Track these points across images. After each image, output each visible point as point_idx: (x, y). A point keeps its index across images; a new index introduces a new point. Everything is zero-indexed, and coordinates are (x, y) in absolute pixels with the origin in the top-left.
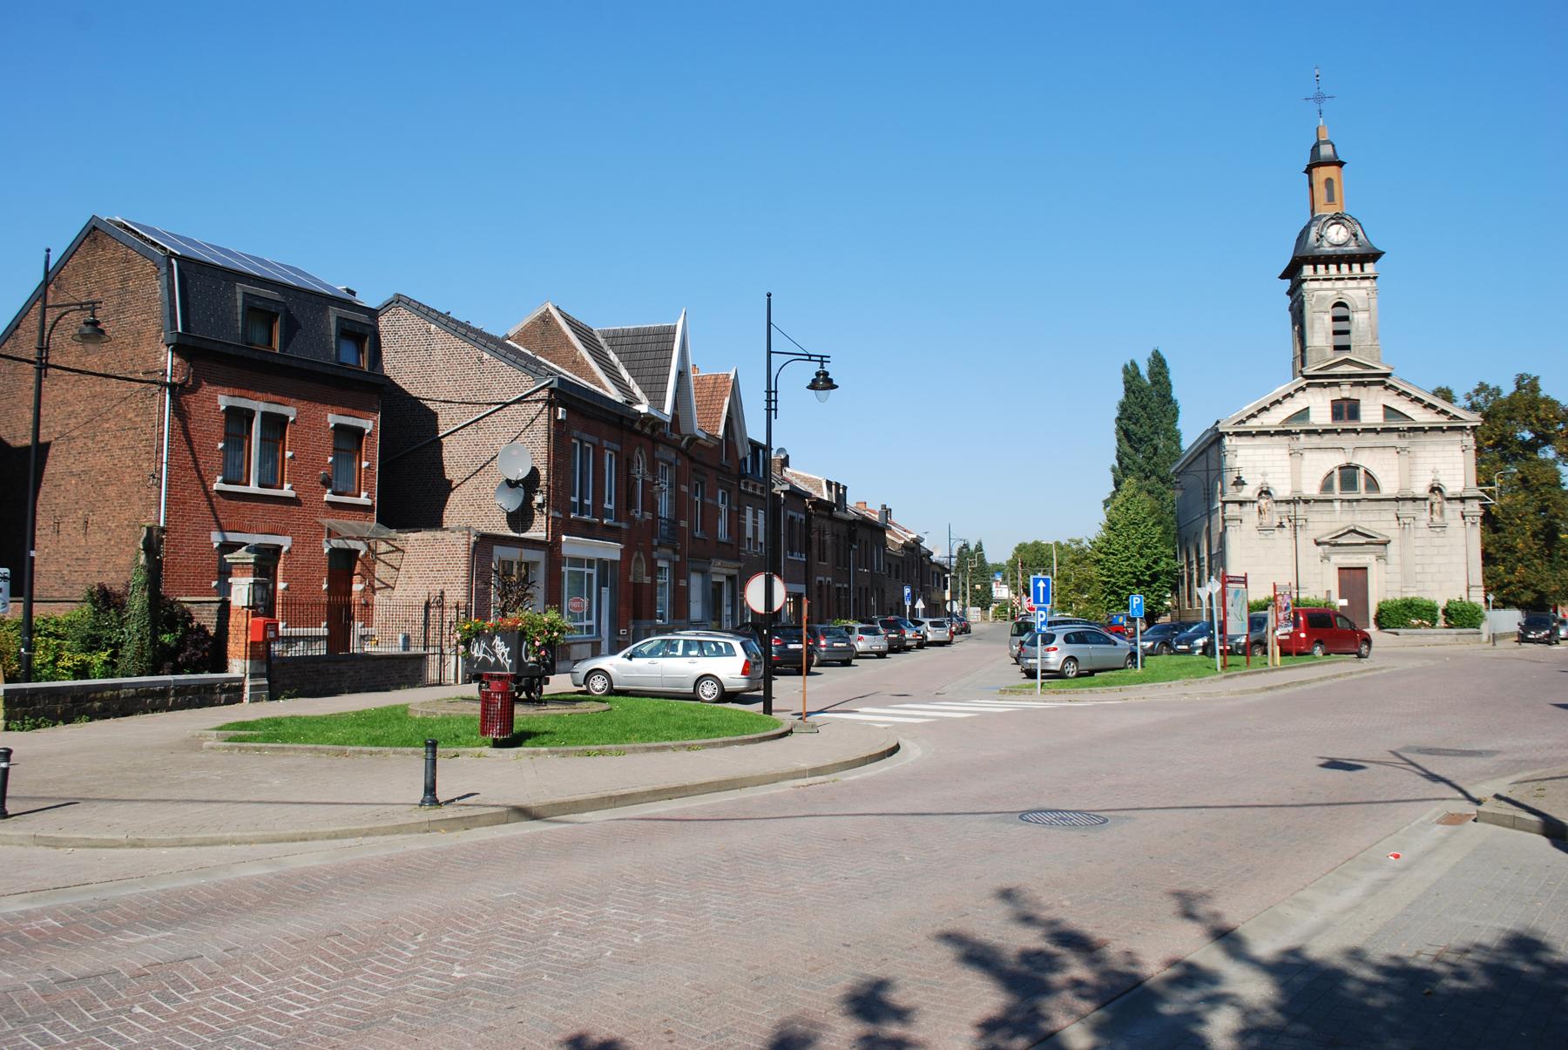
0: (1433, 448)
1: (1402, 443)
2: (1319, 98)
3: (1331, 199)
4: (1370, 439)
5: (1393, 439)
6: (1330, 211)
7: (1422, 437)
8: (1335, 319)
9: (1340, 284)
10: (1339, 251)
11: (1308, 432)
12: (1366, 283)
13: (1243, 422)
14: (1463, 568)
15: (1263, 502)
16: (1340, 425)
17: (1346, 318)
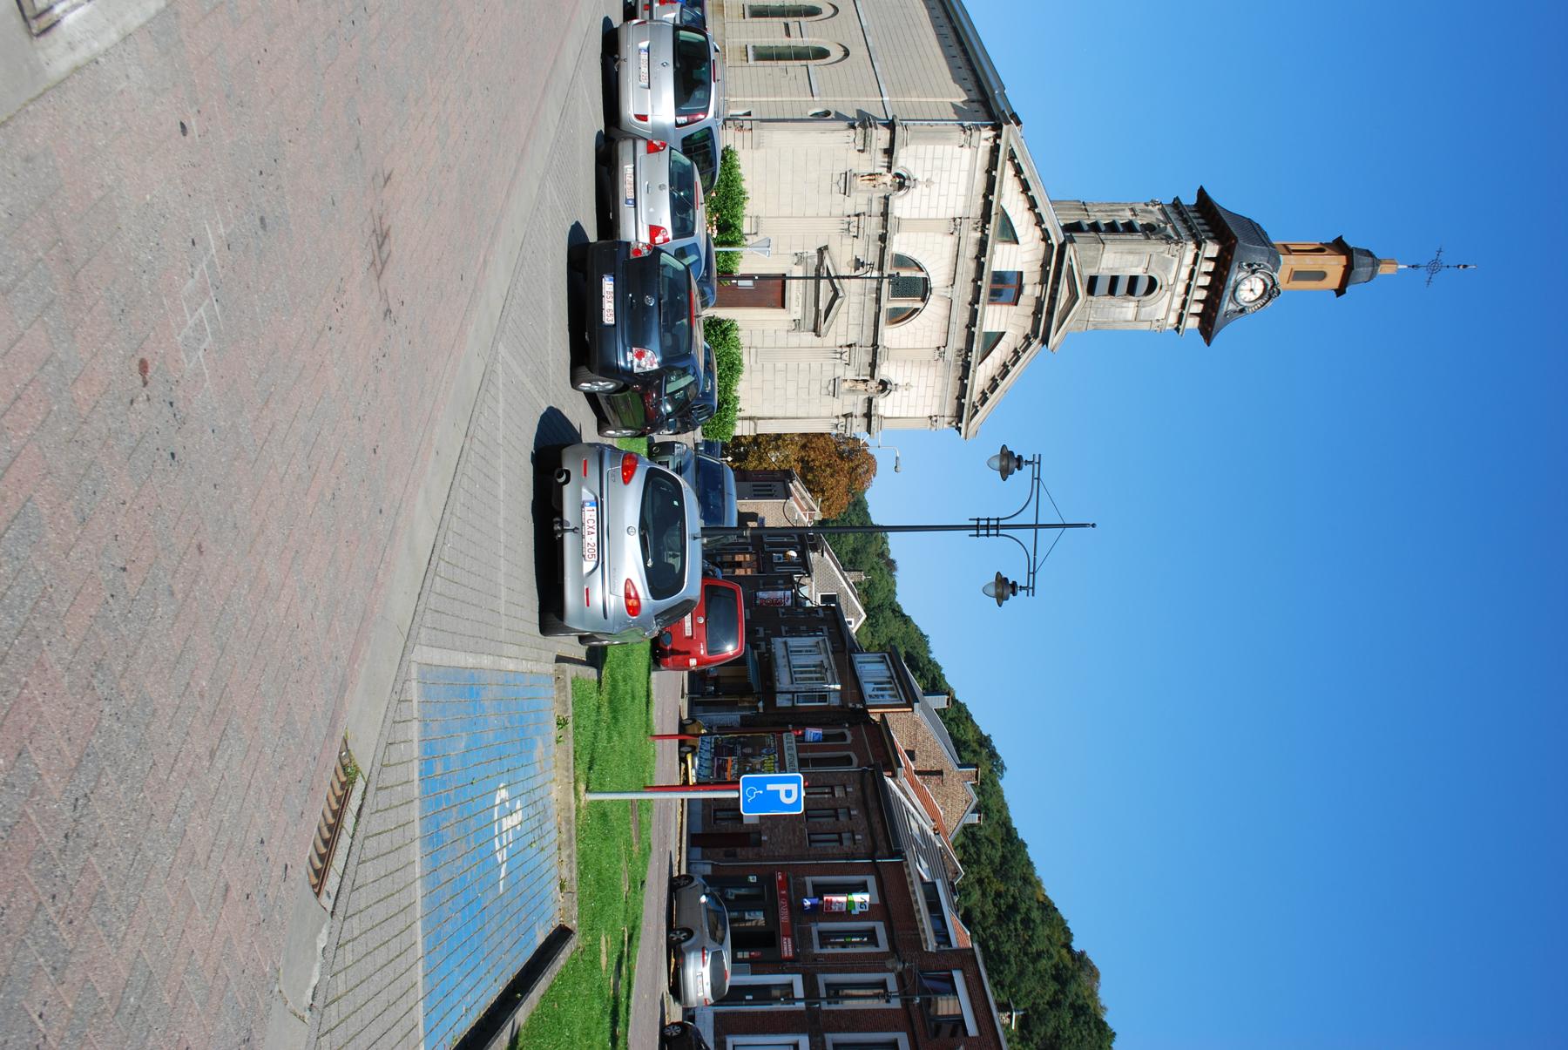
0: (939, 386)
1: (951, 354)
2: (1434, 266)
3: (1298, 275)
4: (961, 317)
5: (957, 342)
6: (1281, 276)
7: (955, 373)
8: (1133, 280)
9: (1181, 288)
10: (1228, 293)
11: (983, 245)
12: (1173, 319)
13: (1012, 157)
14: (779, 413)
15: (888, 178)
16: (986, 284)
17: (1131, 290)
